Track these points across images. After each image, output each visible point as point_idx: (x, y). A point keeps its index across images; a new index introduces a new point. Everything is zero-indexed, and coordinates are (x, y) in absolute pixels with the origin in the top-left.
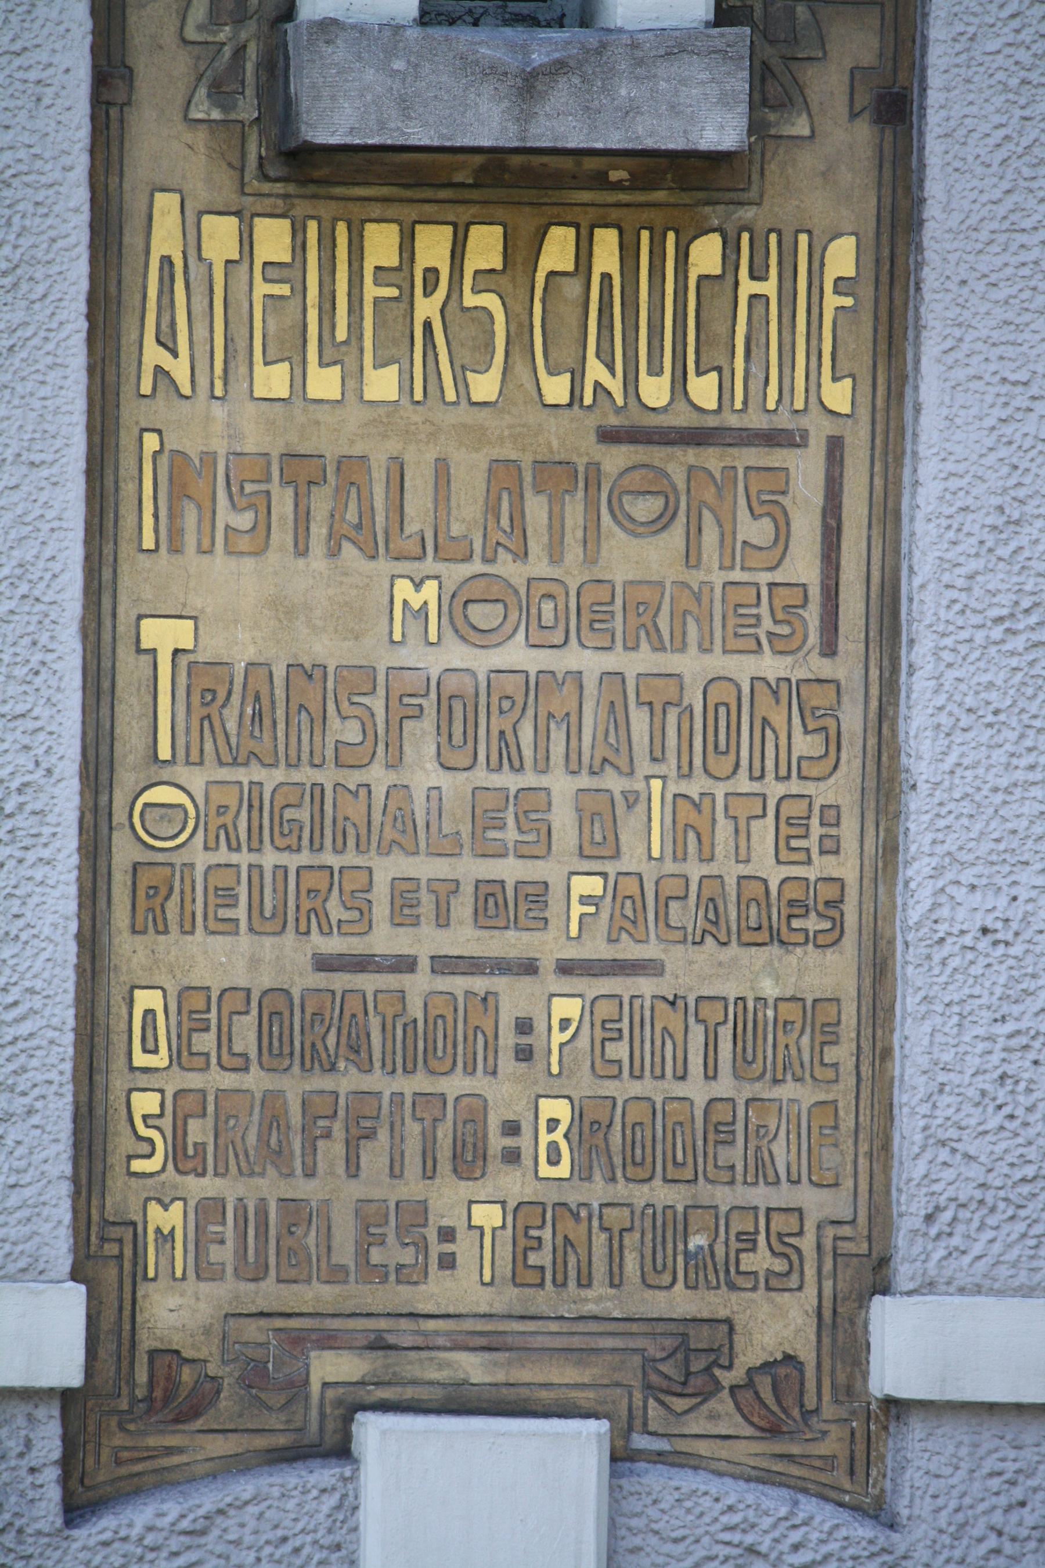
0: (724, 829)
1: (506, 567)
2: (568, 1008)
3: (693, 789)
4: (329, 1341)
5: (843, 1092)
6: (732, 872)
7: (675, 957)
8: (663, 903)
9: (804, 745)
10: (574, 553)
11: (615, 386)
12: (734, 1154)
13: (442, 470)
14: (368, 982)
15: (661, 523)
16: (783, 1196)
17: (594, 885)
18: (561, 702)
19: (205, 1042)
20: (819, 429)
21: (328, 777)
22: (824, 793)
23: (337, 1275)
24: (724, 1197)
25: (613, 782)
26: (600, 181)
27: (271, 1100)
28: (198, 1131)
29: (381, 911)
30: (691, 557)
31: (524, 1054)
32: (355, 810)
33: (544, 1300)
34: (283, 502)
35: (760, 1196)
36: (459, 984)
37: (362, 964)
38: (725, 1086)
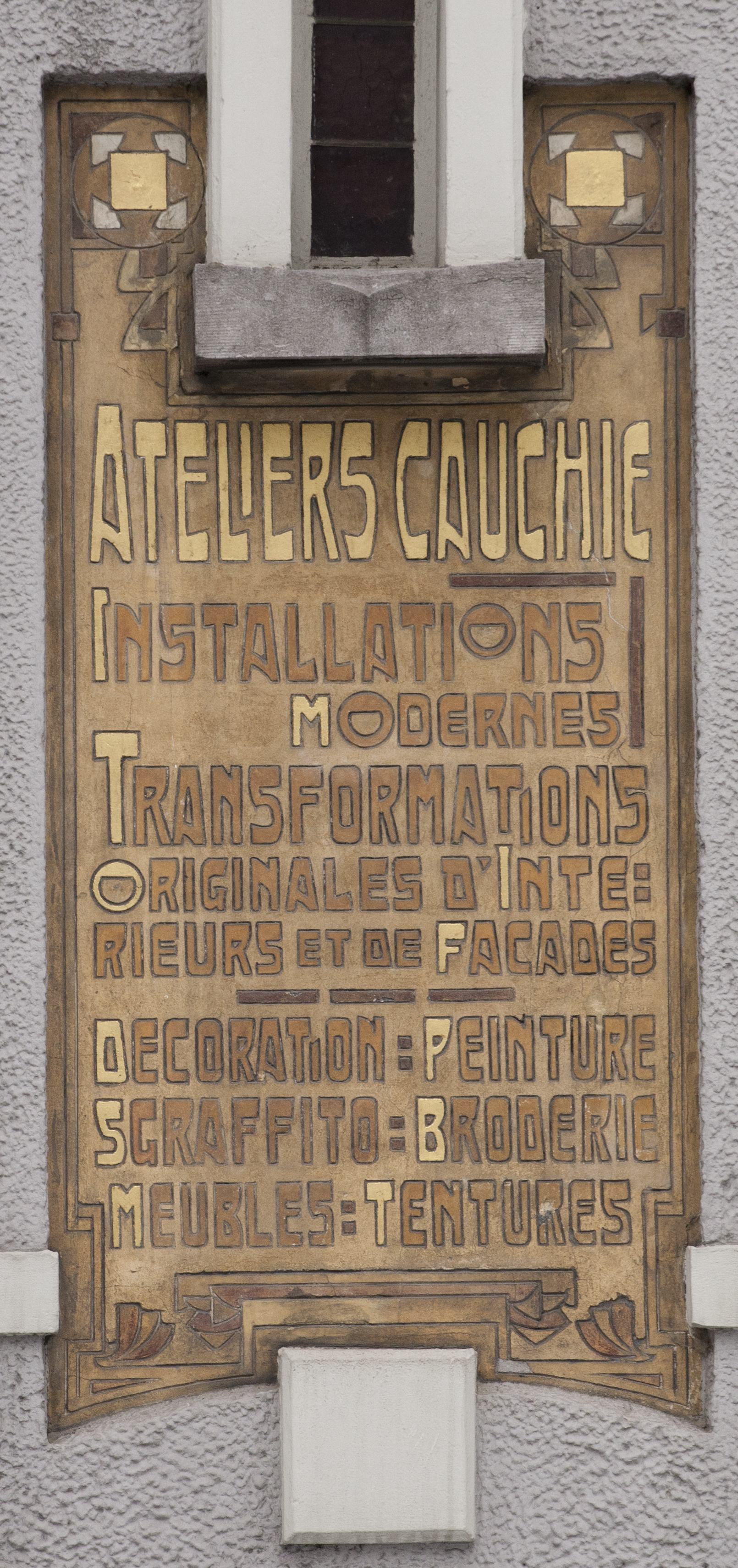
0: (558, 885)
1: (381, 685)
2: (439, 1027)
3: (533, 854)
4: (257, 1293)
5: (659, 1088)
6: (566, 918)
7: (523, 985)
8: (512, 943)
9: (620, 817)
10: (434, 673)
11: (462, 543)
12: (574, 1139)
13: (328, 612)
14: (281, 1011)
15: (501, 648)
16: (614, 1170)
17: (455, 931)
18: (426, 789)
19: (155, 1061)
20: (624, 572)
21: (244, 852)
22: (637, 854)
23: (262, 1241)
24: (566, 1172)
25: (470, 850)
26: (446, 386)
27: (207, 1104)
28: (150, 1131)
29: (290, 955)
30: (526, 673)
31: (405, 1064)
32: (267, 877)
33: (426, 1257)
34: (205, 640)
35: (595, 1171)
36: (352, 1011)
37: (275, 997)
38: (565, 1085)
